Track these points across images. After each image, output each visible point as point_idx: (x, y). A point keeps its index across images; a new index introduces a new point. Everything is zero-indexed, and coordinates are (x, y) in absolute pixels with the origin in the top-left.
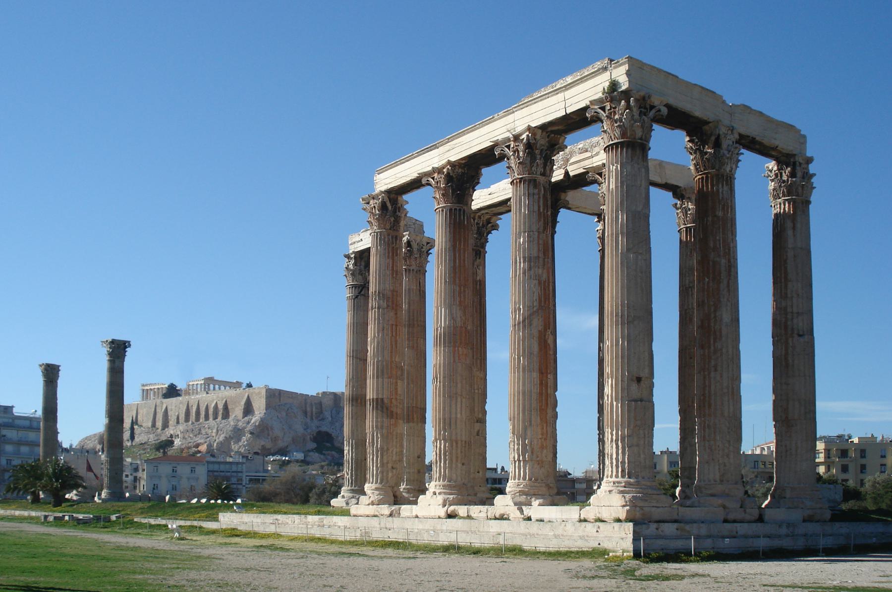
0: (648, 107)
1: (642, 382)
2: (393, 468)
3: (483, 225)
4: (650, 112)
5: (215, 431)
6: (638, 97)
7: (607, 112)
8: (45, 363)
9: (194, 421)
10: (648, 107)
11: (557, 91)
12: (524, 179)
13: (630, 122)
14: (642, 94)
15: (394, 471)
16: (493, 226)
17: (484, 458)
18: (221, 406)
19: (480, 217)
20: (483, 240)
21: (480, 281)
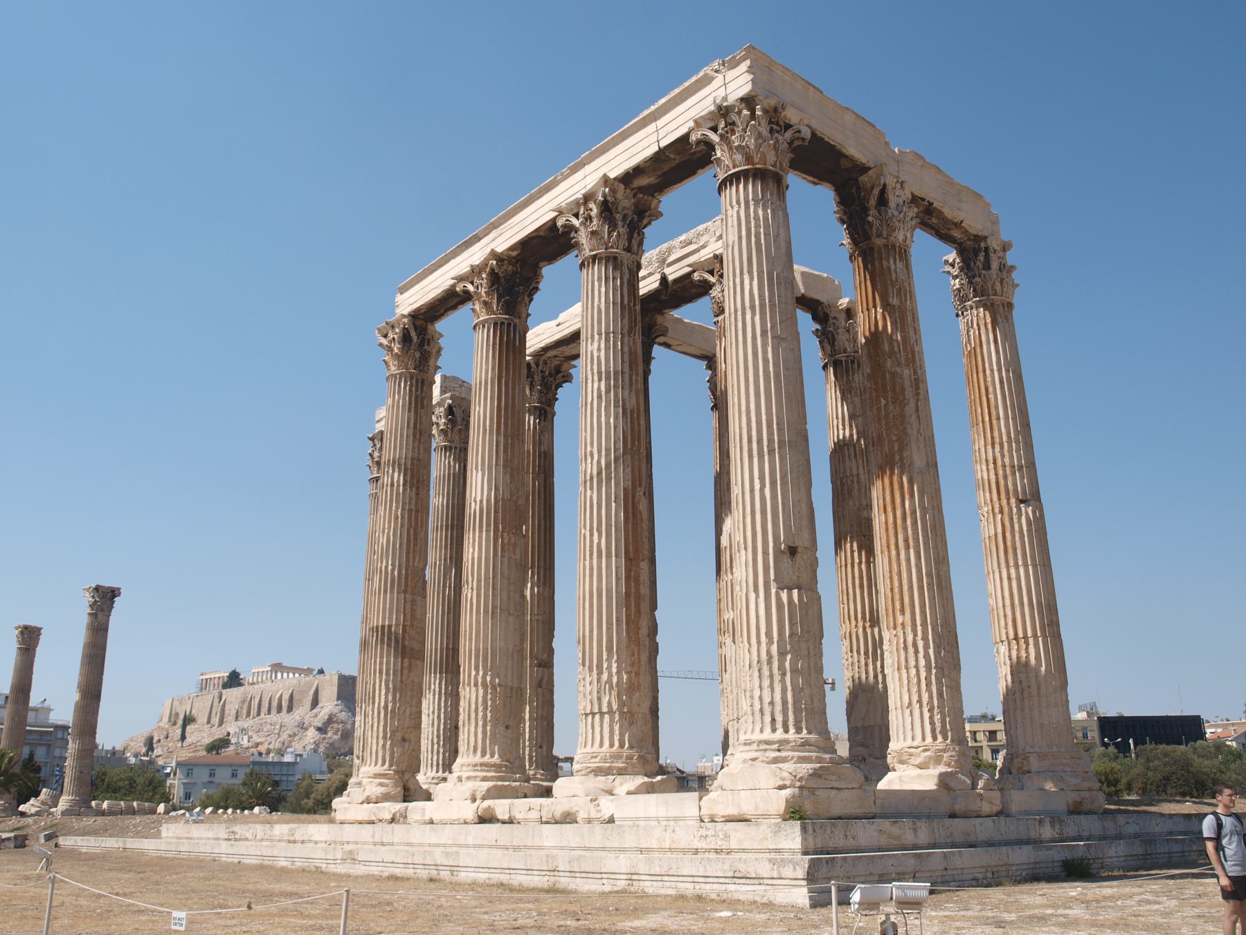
0: (782, 124)
1: (798, 556)
2: (404, 740)
3: (550, 375)
4: (785, 132)
5: (278, 727)
6: (767, 107)
7: (720, 131)
8: (21, 625)
9: (255, 715)
10: (781, 123)
11: (645, 123)
12: (599, 256)
13: (756, 140)
14: (772, 102)
15: (407, 745)
16: (564, 376)
17: (548, 724)
18: (286, 697)
19: (545, 363)
20: (550, 395)
21: (545, 453)
